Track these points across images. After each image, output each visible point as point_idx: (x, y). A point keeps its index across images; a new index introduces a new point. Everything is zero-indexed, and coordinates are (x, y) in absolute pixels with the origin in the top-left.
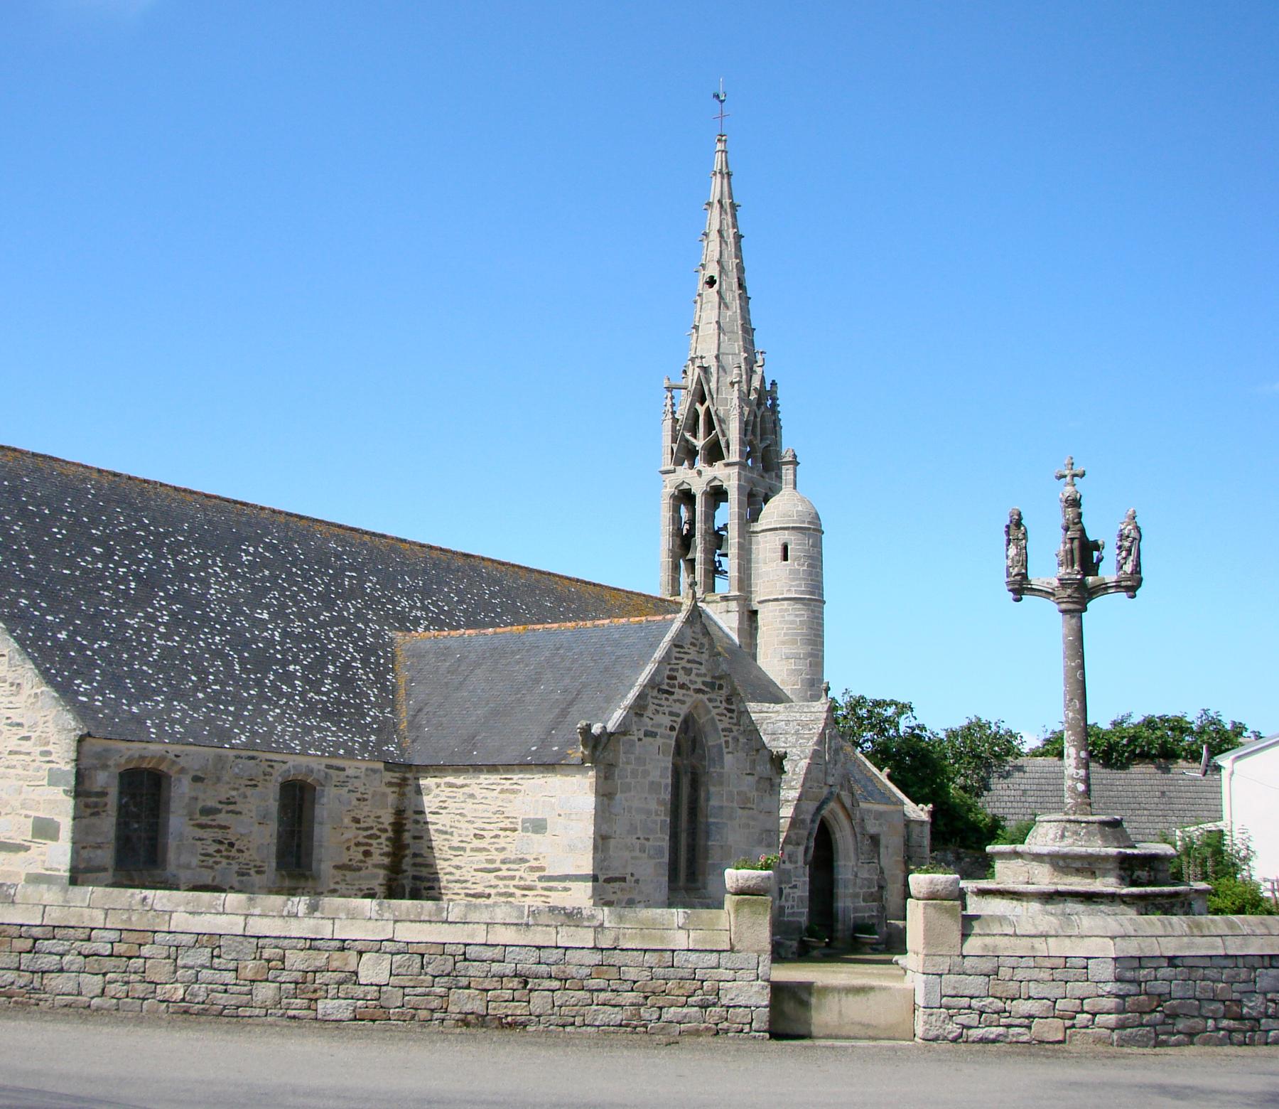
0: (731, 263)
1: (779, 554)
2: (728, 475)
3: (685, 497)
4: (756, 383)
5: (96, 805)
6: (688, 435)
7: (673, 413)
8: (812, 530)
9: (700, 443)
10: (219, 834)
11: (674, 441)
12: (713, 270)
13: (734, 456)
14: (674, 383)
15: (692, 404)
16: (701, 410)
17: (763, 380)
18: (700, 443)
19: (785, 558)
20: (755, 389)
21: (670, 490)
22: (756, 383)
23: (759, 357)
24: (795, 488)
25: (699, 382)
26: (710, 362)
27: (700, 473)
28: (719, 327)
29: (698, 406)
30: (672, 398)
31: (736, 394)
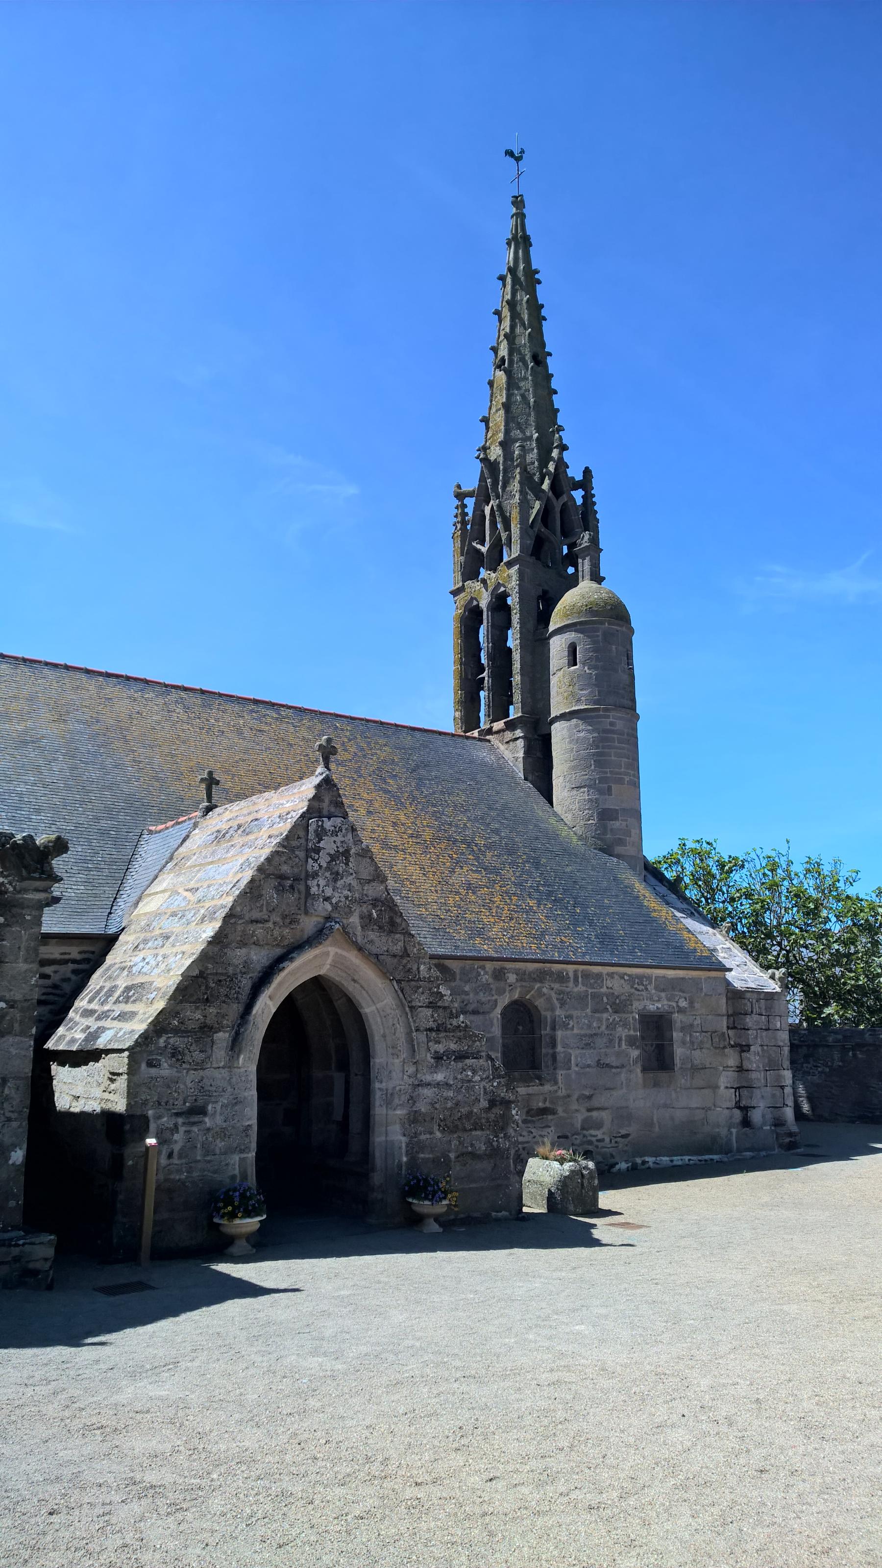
2: (509, 578)
27: (484, 581)
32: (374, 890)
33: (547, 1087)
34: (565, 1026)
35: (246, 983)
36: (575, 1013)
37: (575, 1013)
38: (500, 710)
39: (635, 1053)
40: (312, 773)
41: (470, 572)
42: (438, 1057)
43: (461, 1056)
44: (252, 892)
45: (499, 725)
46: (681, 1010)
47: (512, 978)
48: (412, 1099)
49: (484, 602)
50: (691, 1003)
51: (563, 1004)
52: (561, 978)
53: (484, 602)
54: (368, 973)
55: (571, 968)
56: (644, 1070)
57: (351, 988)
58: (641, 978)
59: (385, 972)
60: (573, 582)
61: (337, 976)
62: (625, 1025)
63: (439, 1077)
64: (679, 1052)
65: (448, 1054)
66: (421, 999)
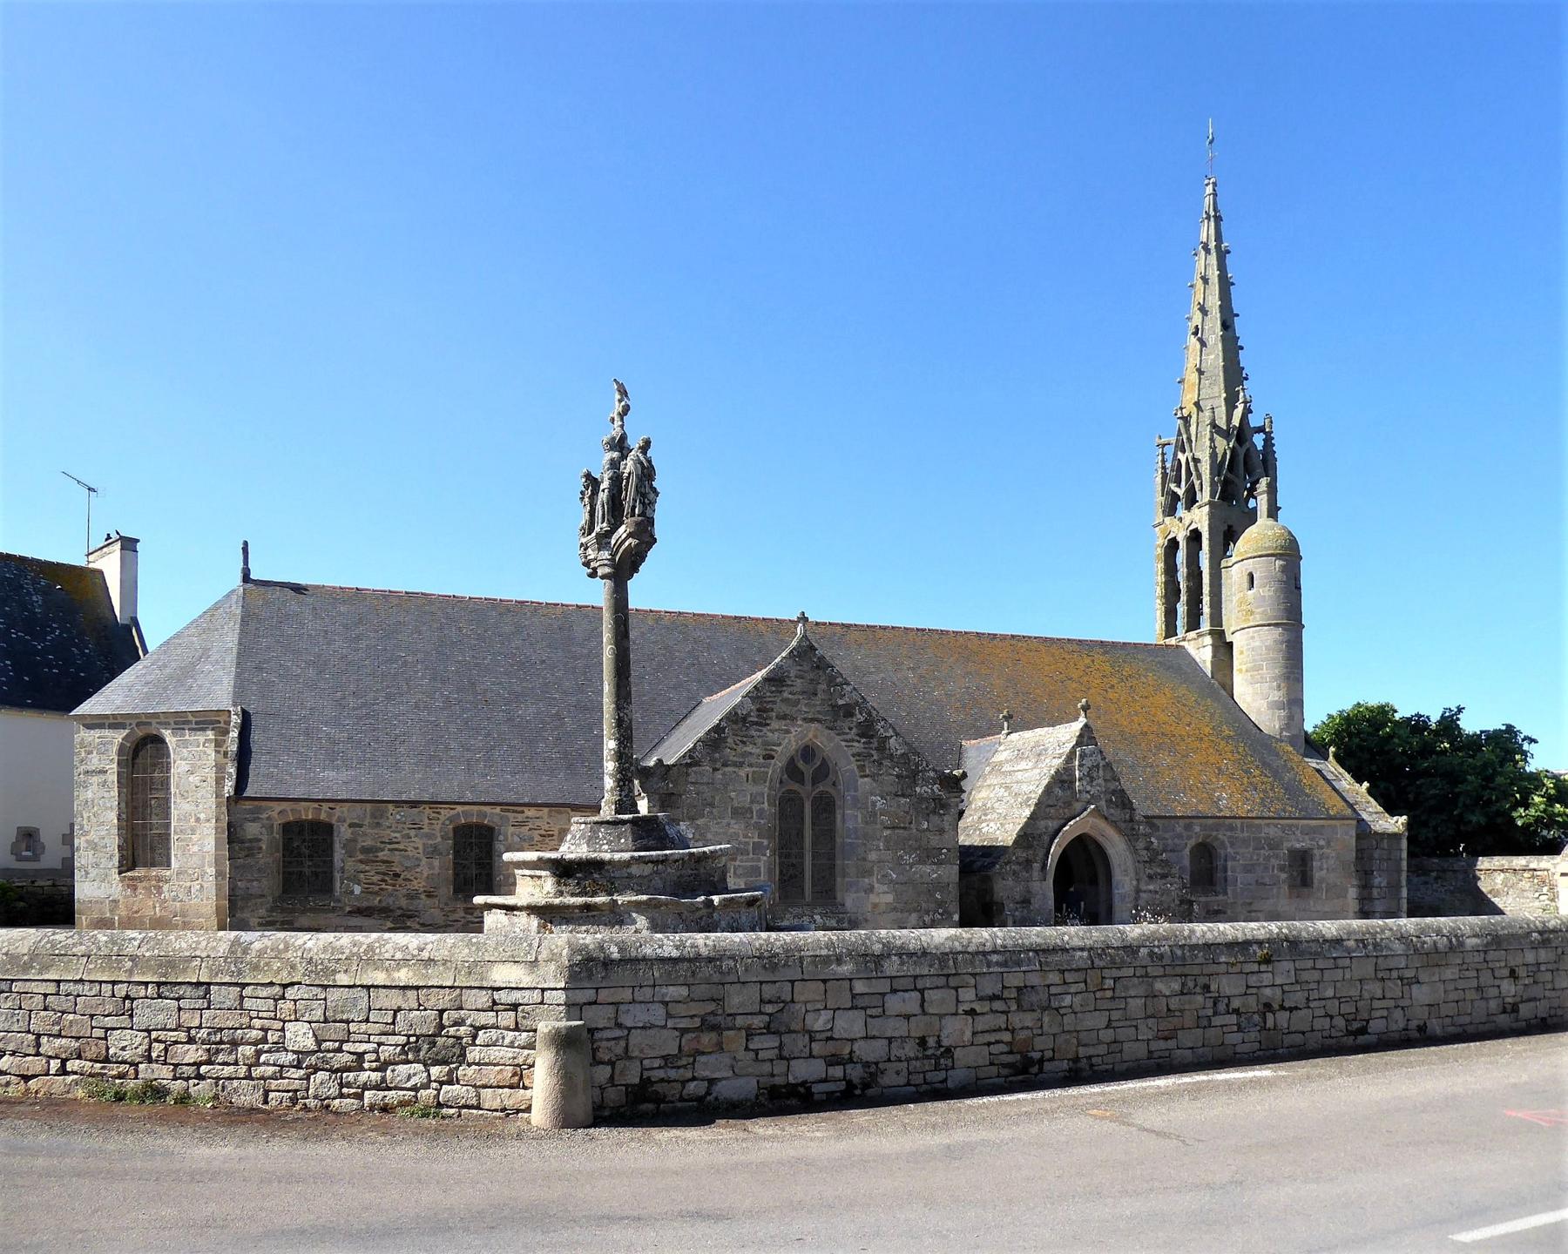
1: (1246, 585)
2: (1199, 518)
3: (1173, 545)
5: (249, 849)
6: (1173, 486)
7: (1164, 468)
8: (1289, 555)
9: (1181, 492)
10: (383, 868)
13: (1204, 496)
15: (1175, 455)
18: (1181, 492)
27: (1181, 519)
29: (1181, 456)
32: (1112, 785)
33: (1221, 897)
34: (1234, 859)
35: (1046, 838)
36: (1241, 851)
37: (1241, 851)
38: (1193, 624)
39: (1284, 876)
40: (1076, 719)
41: (1170, 510)
42: (1150, 877)
43: (1164, 876)
44: (1048, 789)
45: (1192, 634)
46: (1321, 848)
47: (1197, 829)
48: (1136, 899)
49: (1181, 538)
50: (1328, 843)
51: (1232, 844)
52: (1231, 828)
53: (1181, 538)
54: (1110, 832)
55: (1238, 822)
56: (1291, 886)
57: (1101, 839)
58: (1290, 826)
59: (1120, 831)
60: (1251, 517)
61: (1092, 833)
62: (1277, 857)
63: (1151, 887)
64: (1317, 875)
65: (1156, 874)
66: (1141, 844)
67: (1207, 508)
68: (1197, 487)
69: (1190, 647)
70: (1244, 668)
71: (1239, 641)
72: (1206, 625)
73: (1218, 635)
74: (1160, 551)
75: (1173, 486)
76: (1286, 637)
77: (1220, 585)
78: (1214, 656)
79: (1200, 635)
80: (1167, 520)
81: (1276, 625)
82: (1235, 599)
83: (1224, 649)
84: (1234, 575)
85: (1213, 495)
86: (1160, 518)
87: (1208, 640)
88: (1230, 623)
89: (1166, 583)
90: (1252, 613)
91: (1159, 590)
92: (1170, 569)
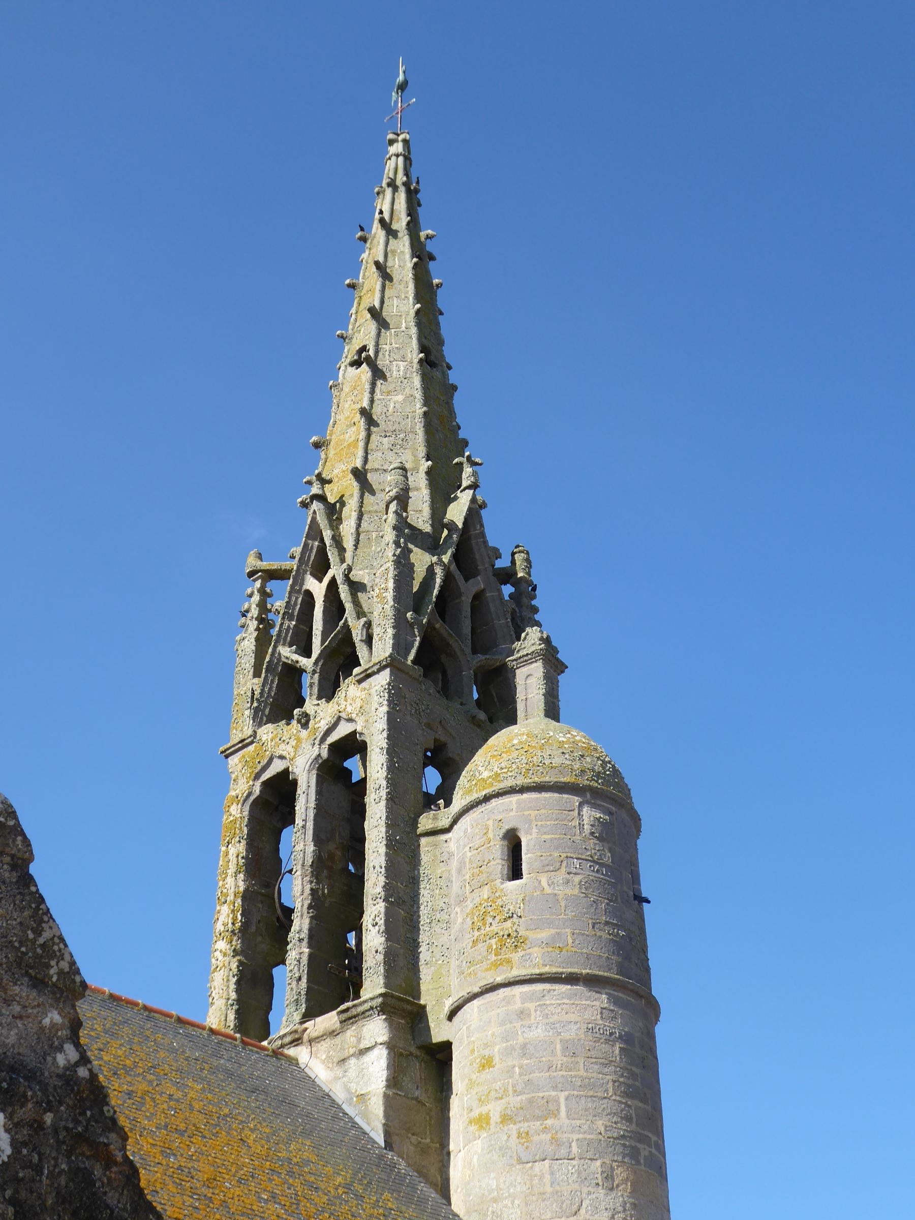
0: (403, 305)
1: (498, 862)
2: (364, 706)
3: (276, 797)
4: (457, 512)
11: (257, 674)
12: (363, 332)
14: (265, 565)
16: (317, 588)
17: (474, 512)
19: (515, 872)
20: (451, 526)
21: (243, 783)
22: (457, 512)
23: (468, 470)
24: (552, 711)
25: (314, 532)
26: (343, 486)
28: (370, 421)
30: (262, 591)
31: (391, 518)
67: (384, 677)
68: (357, 635)
69: (315, 1062)
70: (495, 1109)
71: (472, 1037)
72: (373, 985)
73: (405, 1011)
74: (237, 813)
75: (287, 653)
76: (617, 1026)
77: (414, 881)
78: (393, 1082)
79: (349, 1020)
80: (267, 732)
81: (592, 982)
82: (459, 916)
83: (425, 1065)
84: (460, 851)
85: (400, 645)
86: (243, 726)
87: (376, 1029)
88: (440, 983)
89: (247, 897)
90: (518, 942)
91: (226, 916)
92: (263, 866)
